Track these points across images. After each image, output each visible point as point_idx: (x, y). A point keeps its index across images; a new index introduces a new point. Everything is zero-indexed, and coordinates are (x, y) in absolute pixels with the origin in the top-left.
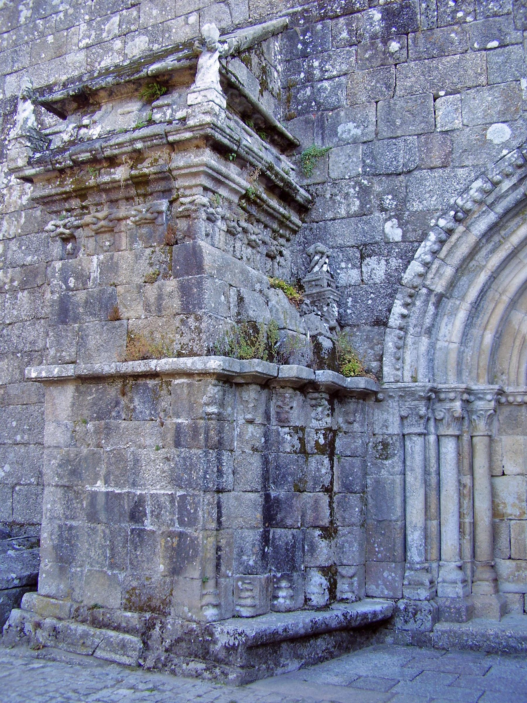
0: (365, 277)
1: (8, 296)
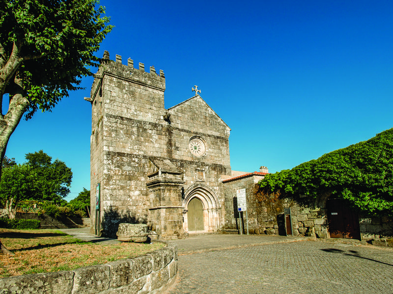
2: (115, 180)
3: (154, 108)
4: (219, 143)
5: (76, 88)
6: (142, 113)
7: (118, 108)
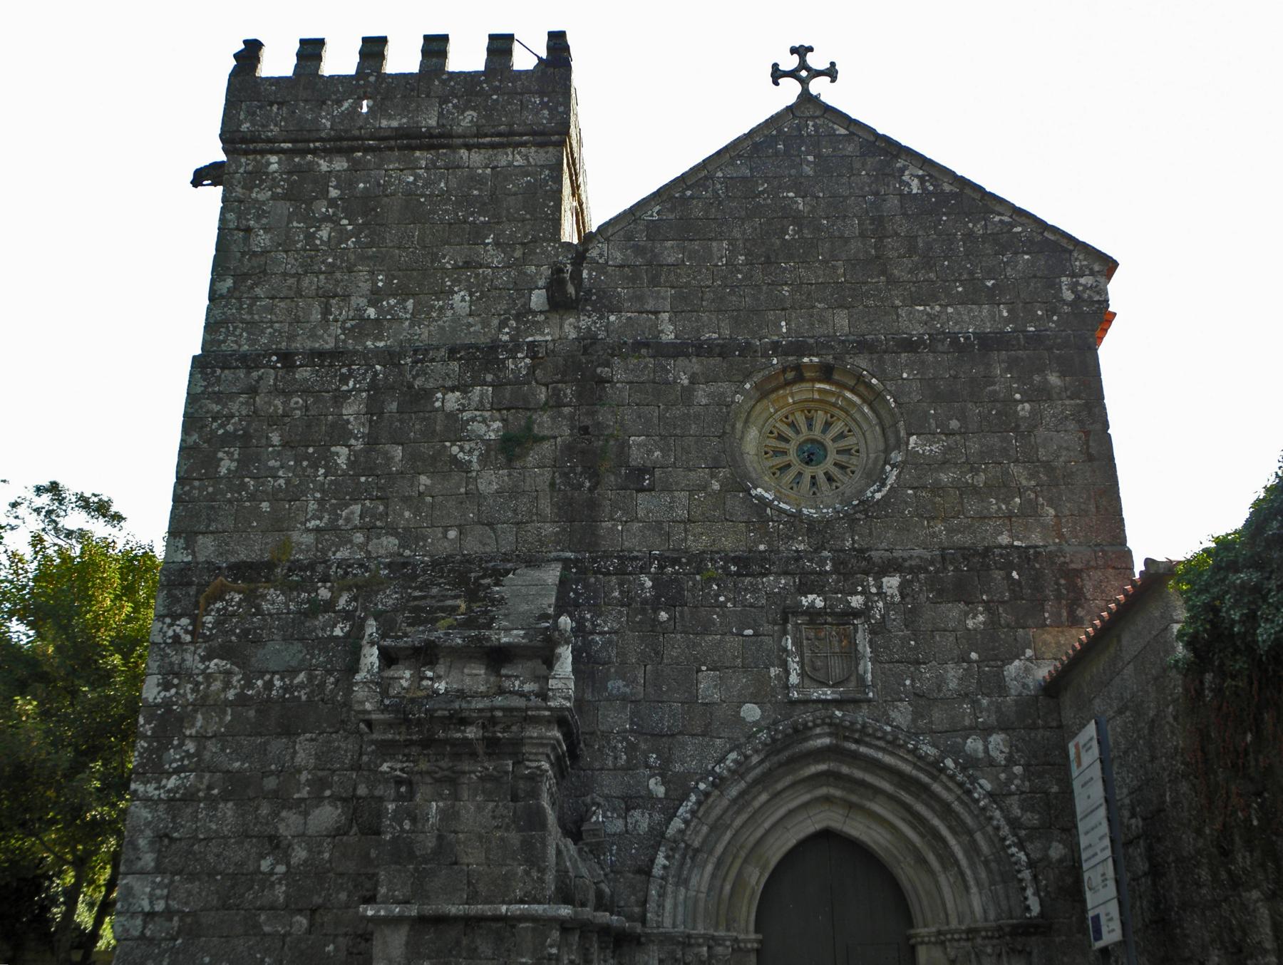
0: (630, 827)
1: (202, 805)
2: (200, 738)
3: (496, 258)
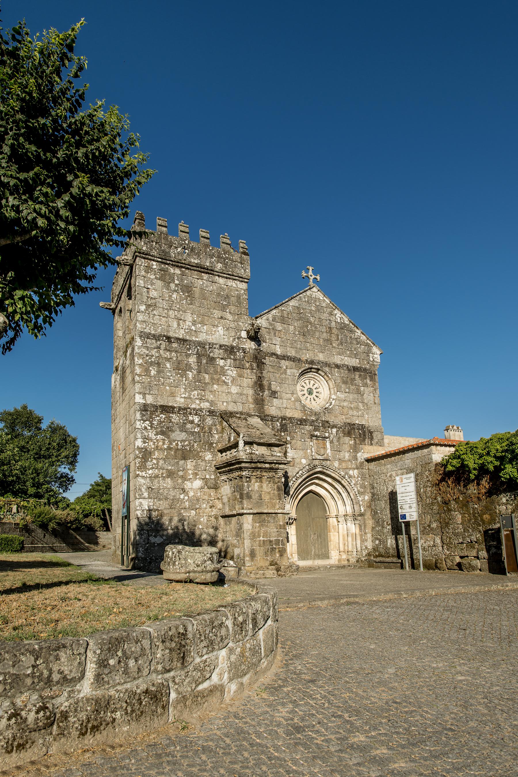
4: (358, 381)
5: (86, 288)
6: (205, 327)
7: (160, 320)
